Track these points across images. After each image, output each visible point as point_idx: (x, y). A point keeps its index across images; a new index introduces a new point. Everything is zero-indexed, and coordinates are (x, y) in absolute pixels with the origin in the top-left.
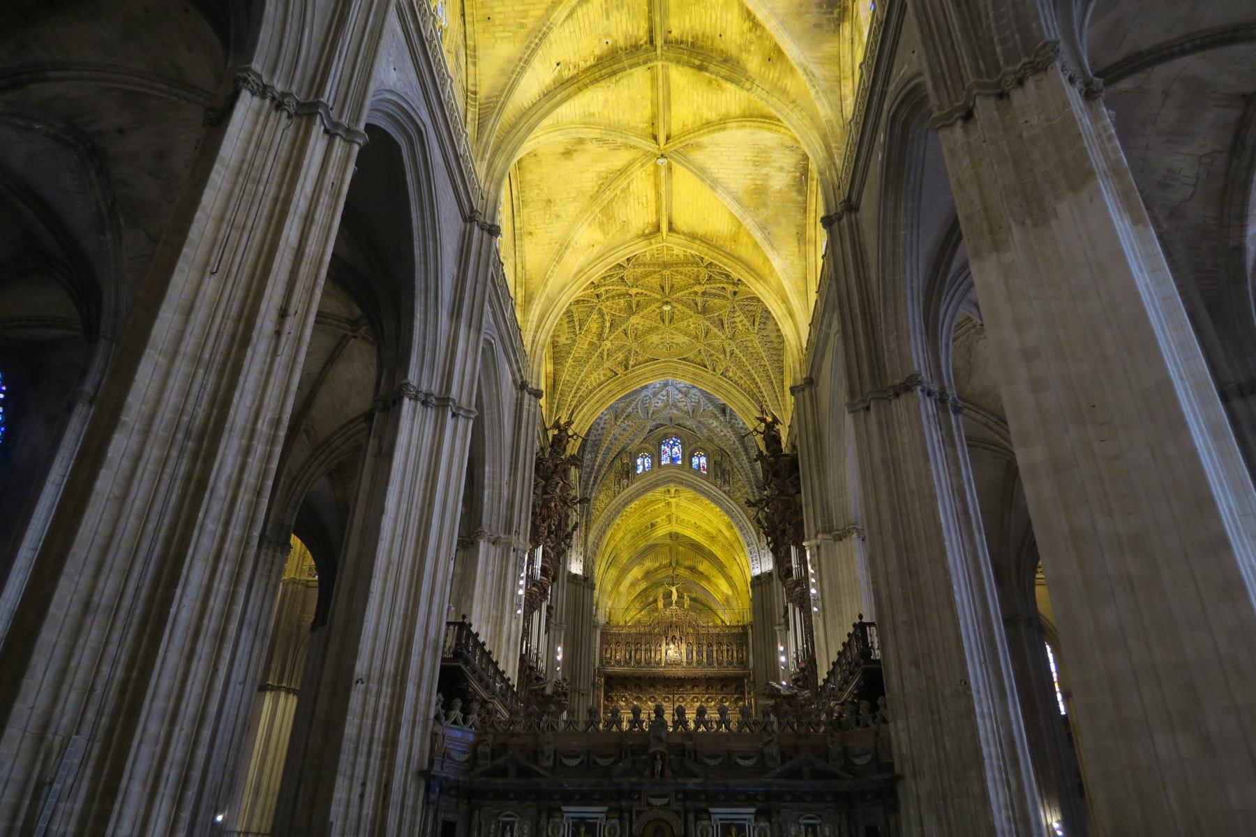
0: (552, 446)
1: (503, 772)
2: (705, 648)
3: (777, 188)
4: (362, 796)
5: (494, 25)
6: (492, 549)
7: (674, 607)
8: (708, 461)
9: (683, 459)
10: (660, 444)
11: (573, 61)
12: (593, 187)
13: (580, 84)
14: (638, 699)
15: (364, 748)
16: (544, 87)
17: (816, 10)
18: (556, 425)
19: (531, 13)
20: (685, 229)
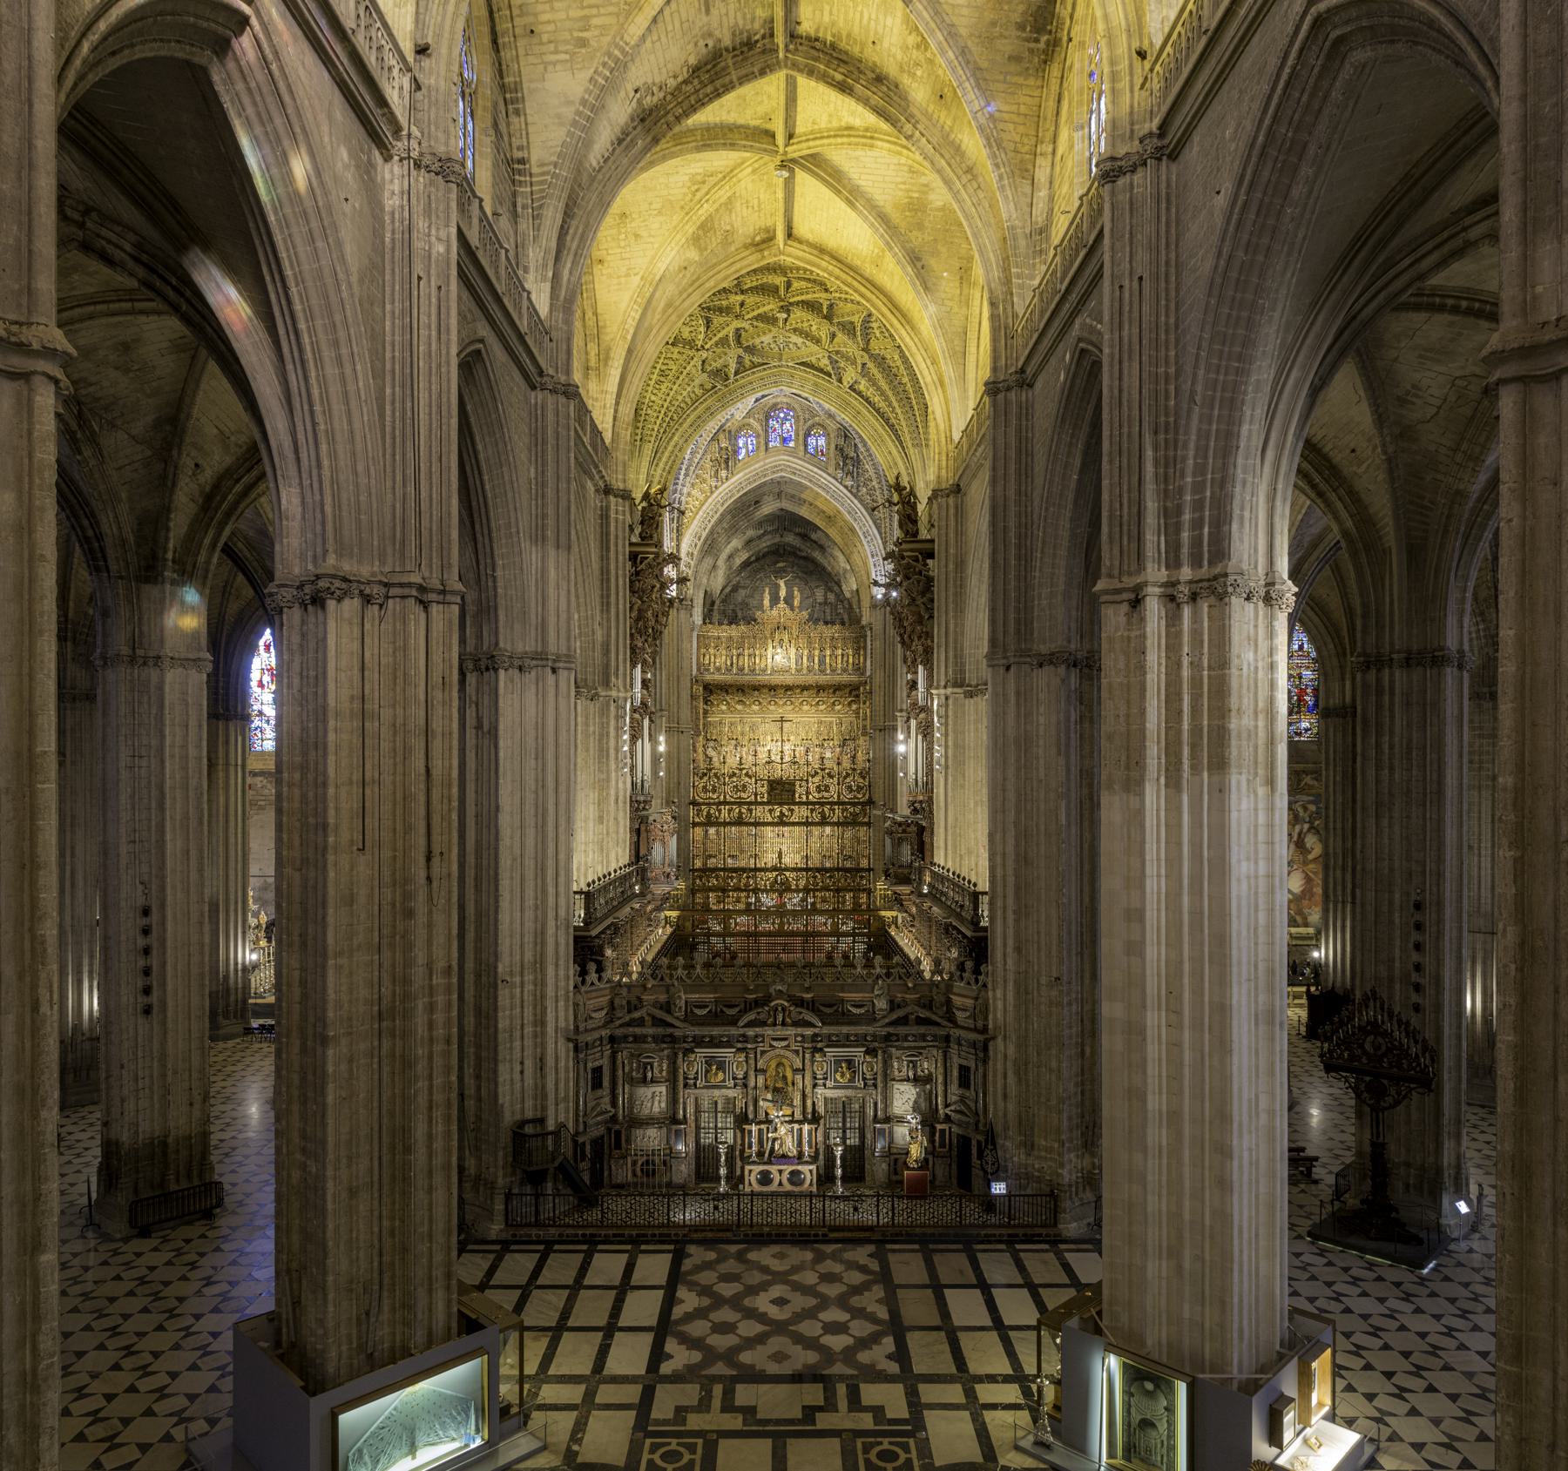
0: (642, 523)
1: (640, 1022)
2: (817, 652)
3: (940, 204)
4: (522, 1072)
5: (541, 44)
6: (591, 705)
7: (782, 605)
8: (828, 444)
9: (797, 440)
10: (768, 417)
11: (657, 81)
12: (685, 194)
13: (670, 118)
14: (740, 702)
15: (518, 1033)
16: (618, 130)
17: (1014, 33)
18: (646, 496)
19: (595, 21)
20: (810, 237)
